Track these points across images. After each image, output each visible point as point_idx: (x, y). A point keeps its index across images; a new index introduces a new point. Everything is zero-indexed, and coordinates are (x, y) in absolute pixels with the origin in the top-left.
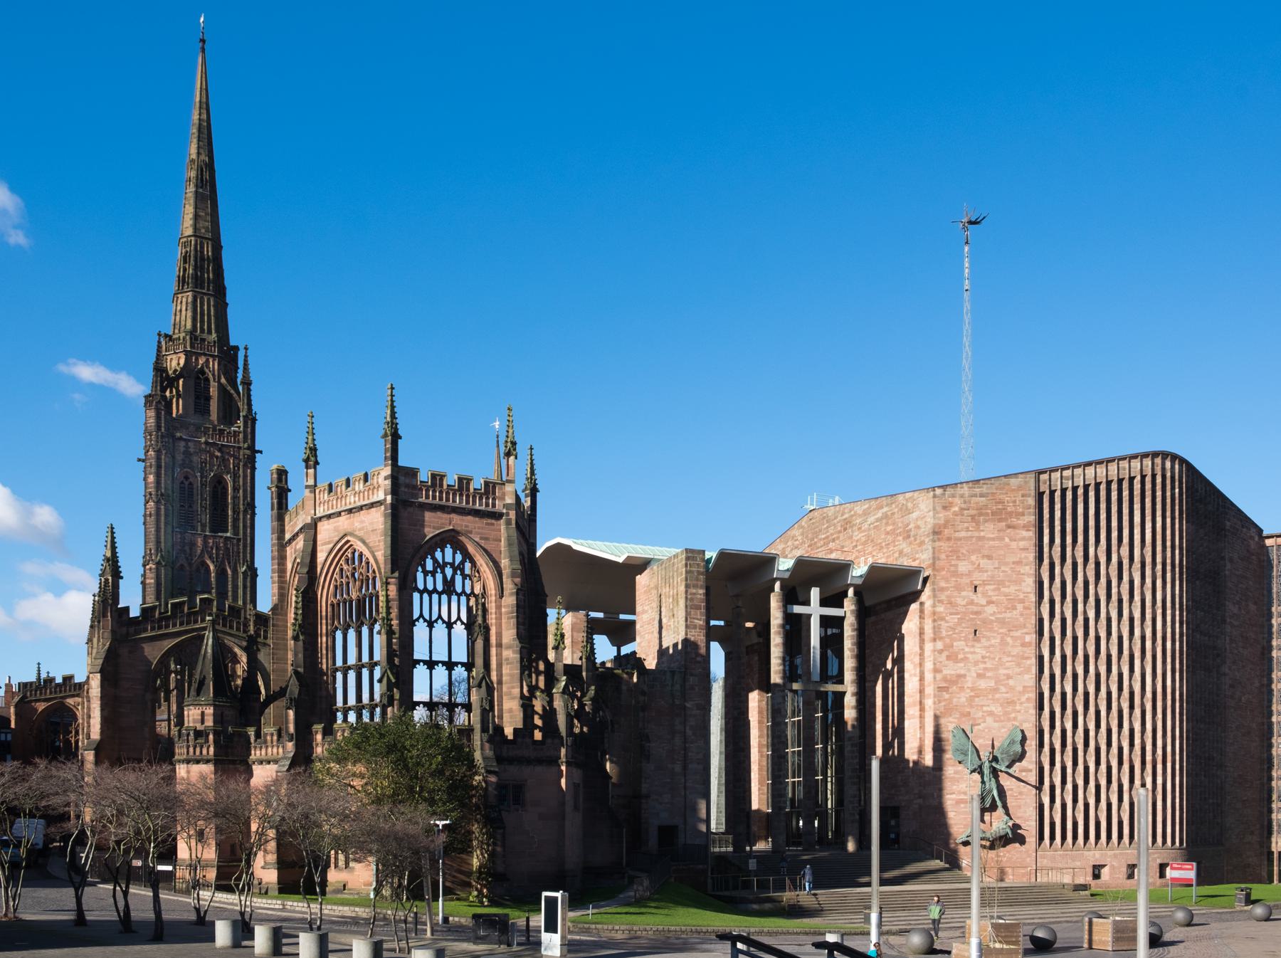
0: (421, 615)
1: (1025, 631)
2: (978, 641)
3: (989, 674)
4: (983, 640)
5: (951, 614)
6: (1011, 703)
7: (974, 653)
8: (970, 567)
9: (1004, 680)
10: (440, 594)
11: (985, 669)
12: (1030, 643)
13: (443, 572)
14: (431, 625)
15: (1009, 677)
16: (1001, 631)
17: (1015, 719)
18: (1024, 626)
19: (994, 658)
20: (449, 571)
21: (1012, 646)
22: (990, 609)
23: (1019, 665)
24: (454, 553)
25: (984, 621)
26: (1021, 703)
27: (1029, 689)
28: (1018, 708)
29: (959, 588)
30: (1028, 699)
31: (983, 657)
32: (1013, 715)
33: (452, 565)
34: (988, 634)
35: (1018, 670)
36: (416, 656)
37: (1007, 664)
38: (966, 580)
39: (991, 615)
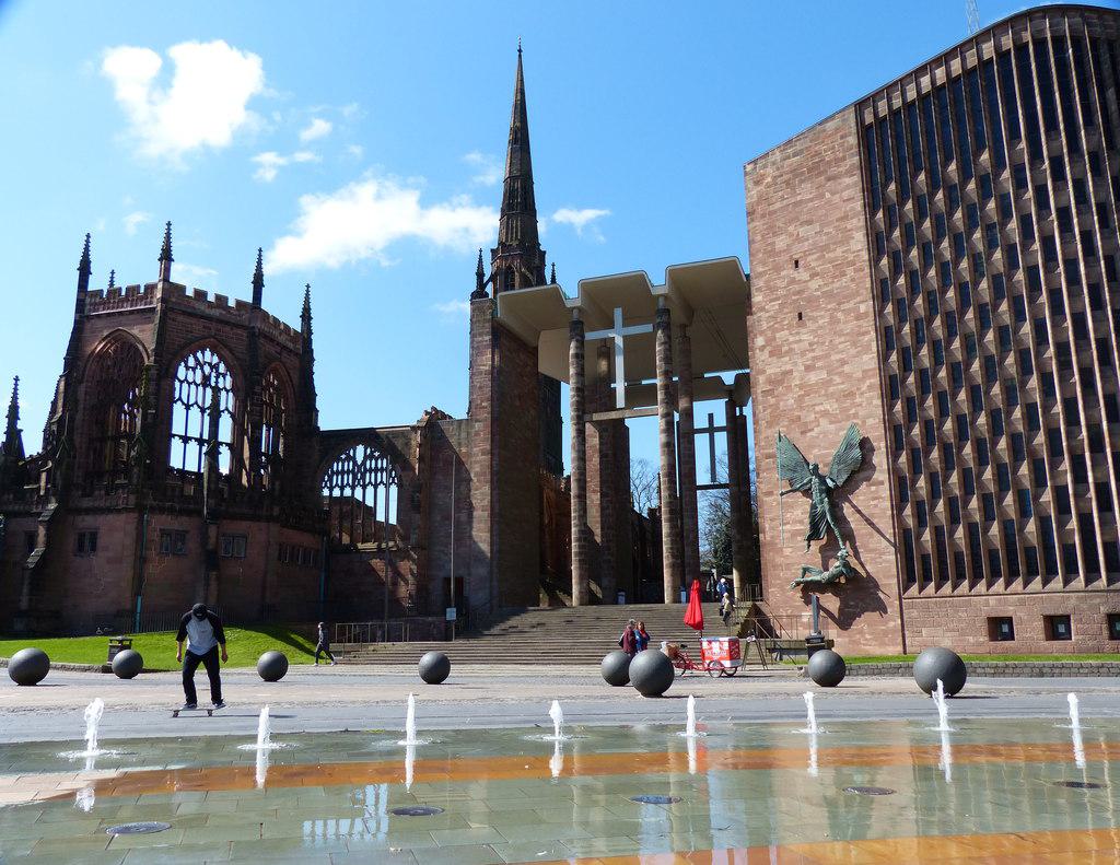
0: (180, 399)
1: (858, 299)
2: (804, 325)
3: (819, 364)
4: (809, 324)
5: (771, 301)
6: (851, 395)
7: (800, 341)
8: (789, 241)
9: (837, 368)
10: (197, 385)
11: (814, 358)
12: (866, 314)
13: (202, 369)
14: (188, 407)
15: (843, 362)
16: (829, 307)
17: (855, 416)
18: (857, 293)
19: (823, 343)
20: (207, 369)
21: (846, 322)
22: (814, 284)
23: (854, 344)
24: (212, 355)
25: (810, 300)
26: (862, 394)
27: (870, 373)
28: (858, 400)
29: (777, 269)
30: (870, 387)
31: (811, 345)
32: (853, 411)
33: (210, 364)
34: (815, 314)
35: (853, 351)
36: (174, 432)
37: (840, 346)
38: (785, 257)
39: (817, 290)
